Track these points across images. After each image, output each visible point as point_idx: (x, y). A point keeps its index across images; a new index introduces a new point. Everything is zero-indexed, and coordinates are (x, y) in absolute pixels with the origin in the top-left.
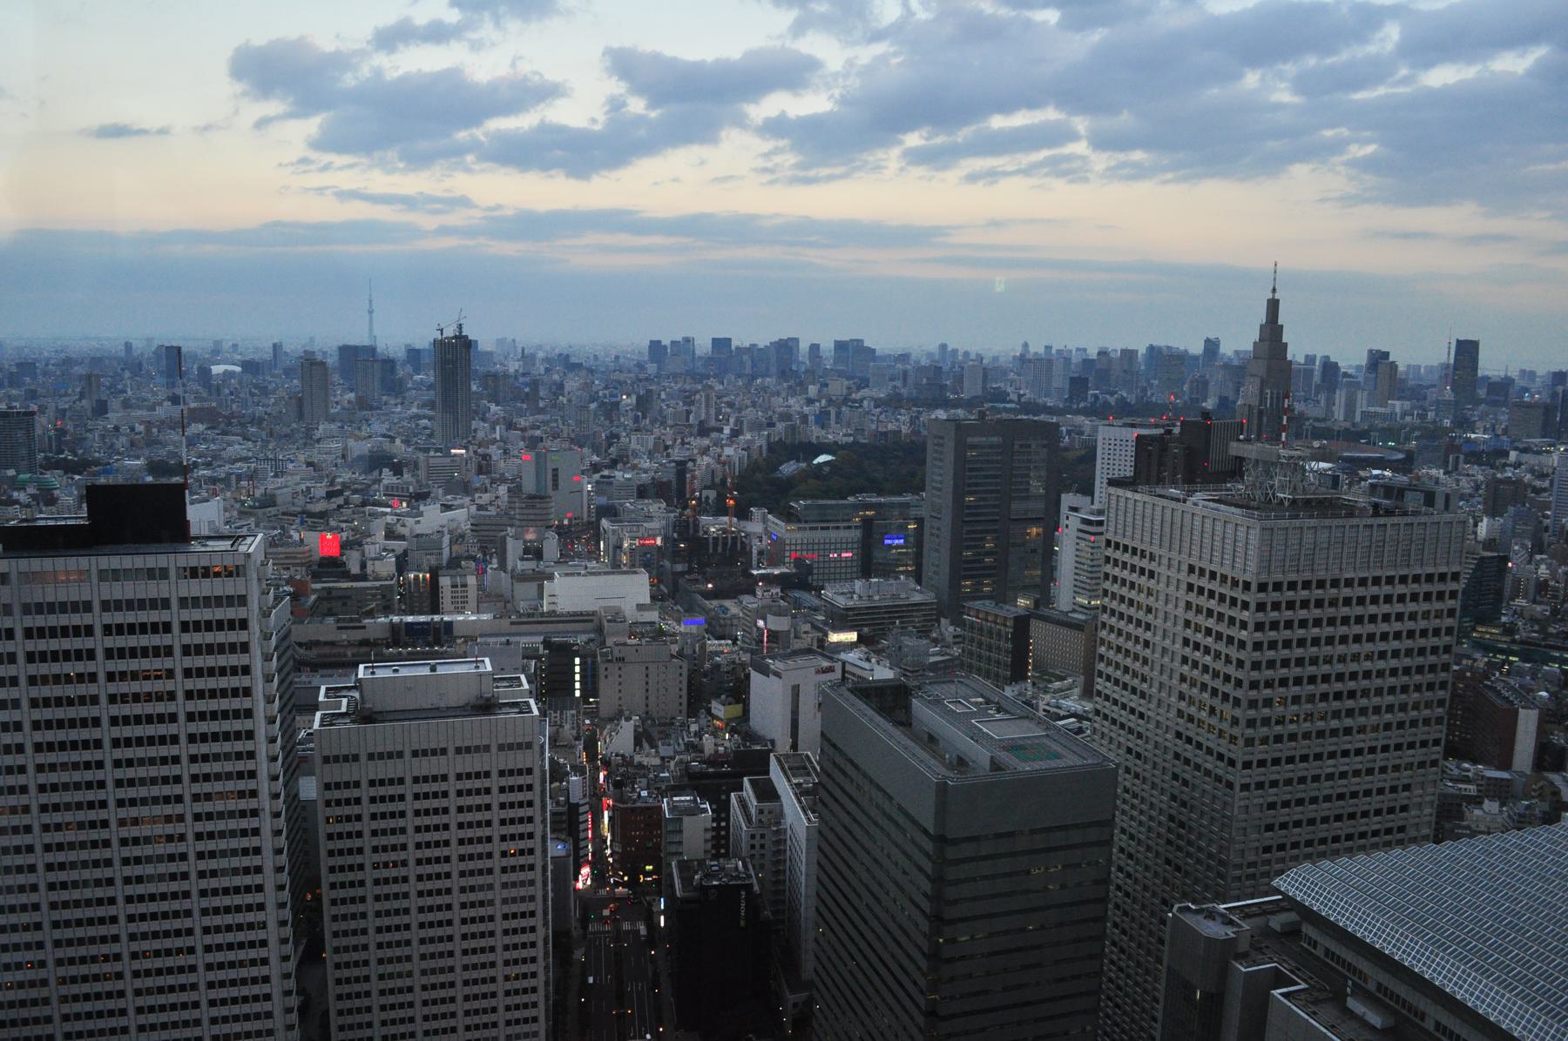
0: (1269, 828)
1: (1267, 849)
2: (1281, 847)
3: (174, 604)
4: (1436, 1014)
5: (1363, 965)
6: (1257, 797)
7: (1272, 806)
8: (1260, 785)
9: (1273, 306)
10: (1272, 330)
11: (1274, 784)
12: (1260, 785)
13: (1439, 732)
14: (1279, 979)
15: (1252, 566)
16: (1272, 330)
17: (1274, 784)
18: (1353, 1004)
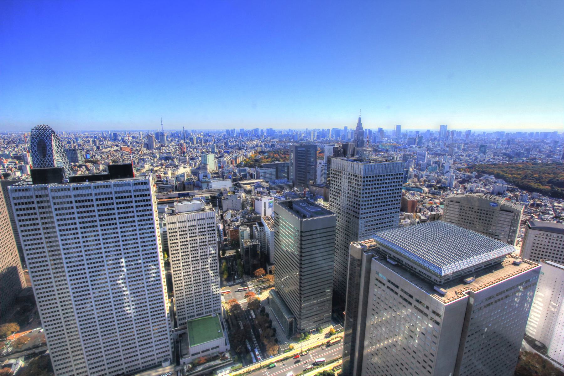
0: (366, 226)
1: (366, 231)
2: (369, 230)
3: (132, 191)
4: (405, 261)
5: (390, 252)
6: (364, 221)
7: (367, 222)
8: (364, 218)
9: (360, 119)
10: (360, 124)
11: (367, 217)
12: (364, 218)
13: (400, 206)
14: (373, 256)
15: (362, 173)
16: (360, 124)
17: (367, 217)
18: (388, 260)
